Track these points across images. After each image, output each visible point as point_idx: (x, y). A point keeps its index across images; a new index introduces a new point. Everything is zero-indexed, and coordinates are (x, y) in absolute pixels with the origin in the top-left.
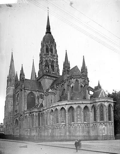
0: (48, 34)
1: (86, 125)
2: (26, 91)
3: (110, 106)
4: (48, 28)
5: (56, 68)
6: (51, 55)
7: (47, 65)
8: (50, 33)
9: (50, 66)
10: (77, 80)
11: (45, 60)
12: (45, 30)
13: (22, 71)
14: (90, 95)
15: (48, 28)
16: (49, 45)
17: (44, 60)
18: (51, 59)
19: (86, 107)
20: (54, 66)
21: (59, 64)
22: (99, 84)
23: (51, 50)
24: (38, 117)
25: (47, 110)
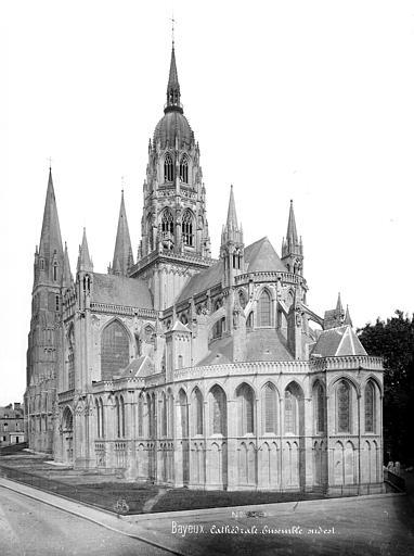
0: (170, 115)
2: (98, 316)
3: (372, 381)
4: (173, 92)
5: (197, 235)
6: (181, 188)
7: (169, 226)
8: (180, 111)
9: (179, 229)
10: (266, 290)
11: (161, 207)
12: (163, 101)
13: (83, 249)
14: (316, 318)
15: (173, 92)
16: (174, 151)
17: (158, 205)
18: (182, 204)
19: (293, 388)
21: (208, 216)
22: (339, 303)
23: (184, 171)
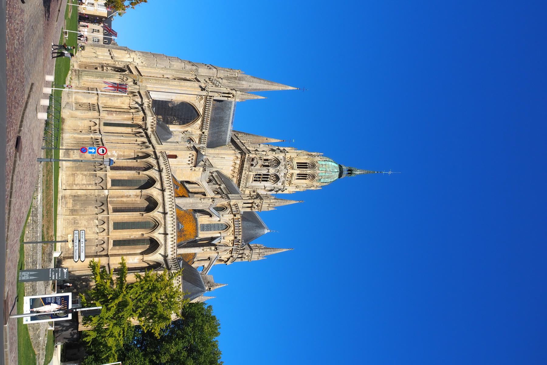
1: (105, 246)
9: (264, 171)
10: (227, 227)
11: (279, 159)
19: (154, 245)
20: (267, 181)
24: (130, 122)
25: (150, 145)
